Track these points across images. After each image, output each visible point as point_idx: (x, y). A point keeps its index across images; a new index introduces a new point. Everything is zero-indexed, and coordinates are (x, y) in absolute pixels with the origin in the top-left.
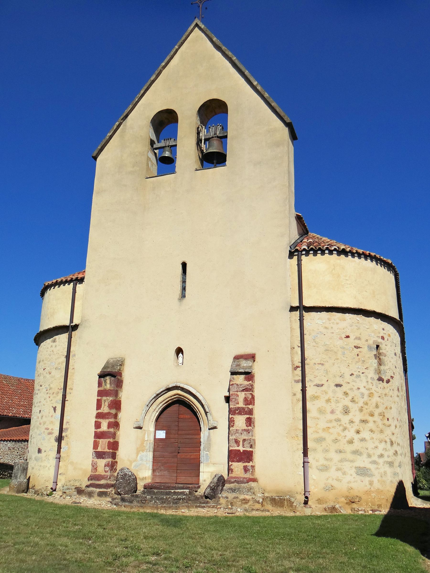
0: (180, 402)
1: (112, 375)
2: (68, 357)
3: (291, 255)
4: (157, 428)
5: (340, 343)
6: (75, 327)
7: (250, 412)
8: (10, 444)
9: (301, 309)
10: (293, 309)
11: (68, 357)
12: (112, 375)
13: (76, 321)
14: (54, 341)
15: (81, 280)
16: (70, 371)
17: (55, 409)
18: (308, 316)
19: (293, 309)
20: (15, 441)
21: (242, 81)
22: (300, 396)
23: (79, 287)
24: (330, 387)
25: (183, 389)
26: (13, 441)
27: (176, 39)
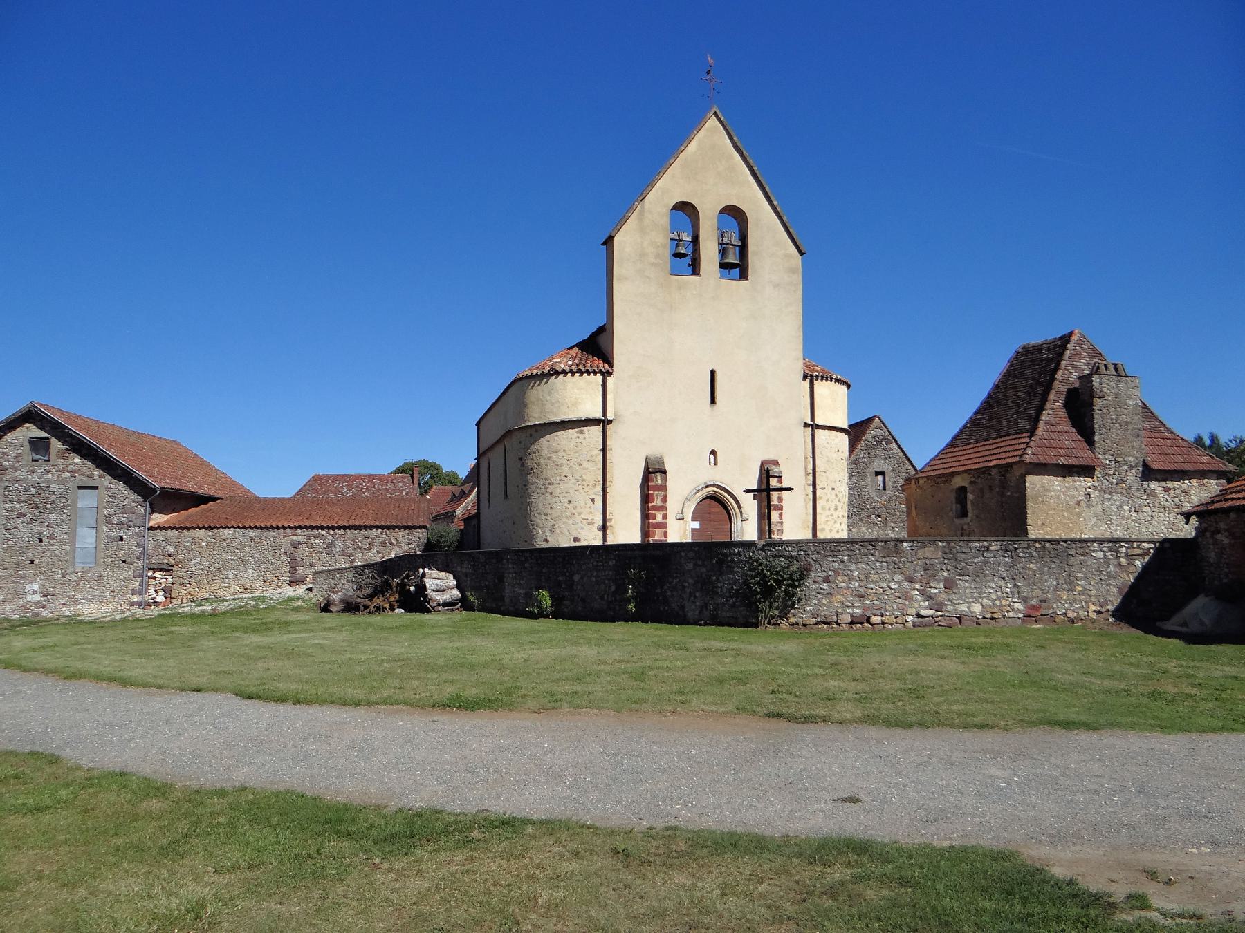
0: (712, 497)
1: (653, 474)
2: (604, 450)
3: (805, 377)
4: (694, 519)
5: (834, 455)
6: (610, 422)
7: (781, 509)
8: (251, 533)
9: (814, 427)
10: (806, 425)
11: (604, 450)
12: (653, 474)
13: (609, 416)
14: (582, 432)
15: (610, 374)
16: (608, 464)
17: (593, 500)
18: (818, 432)
19: (806, 425)
20: (262, 528)
21: (761, 194)
22: (811, 496)
23: (1032, 483)
24: (828, 490)
25: (719, 487)
26: (257, 528)
27: (695, 124)
